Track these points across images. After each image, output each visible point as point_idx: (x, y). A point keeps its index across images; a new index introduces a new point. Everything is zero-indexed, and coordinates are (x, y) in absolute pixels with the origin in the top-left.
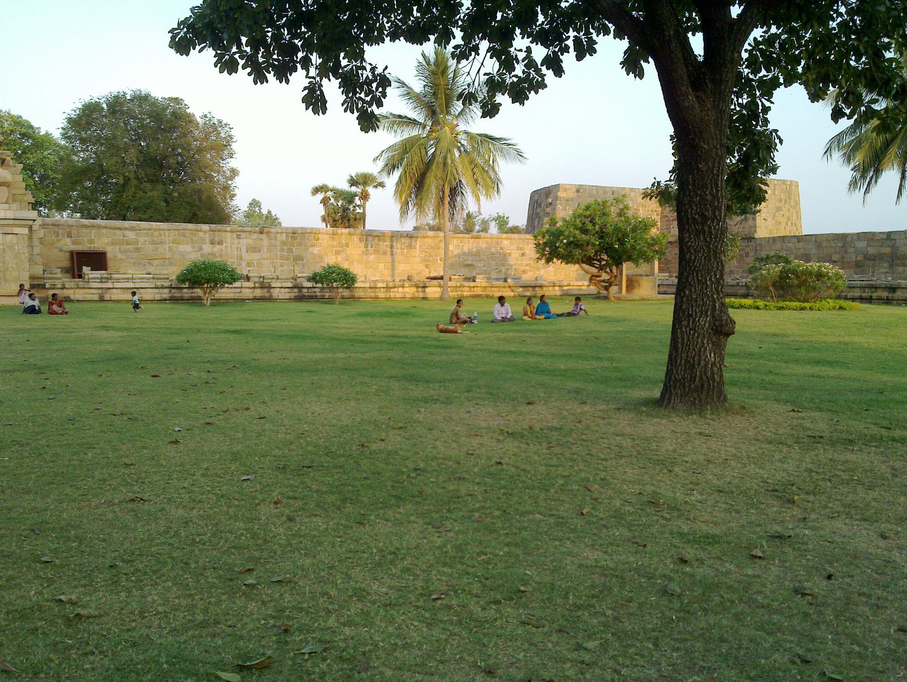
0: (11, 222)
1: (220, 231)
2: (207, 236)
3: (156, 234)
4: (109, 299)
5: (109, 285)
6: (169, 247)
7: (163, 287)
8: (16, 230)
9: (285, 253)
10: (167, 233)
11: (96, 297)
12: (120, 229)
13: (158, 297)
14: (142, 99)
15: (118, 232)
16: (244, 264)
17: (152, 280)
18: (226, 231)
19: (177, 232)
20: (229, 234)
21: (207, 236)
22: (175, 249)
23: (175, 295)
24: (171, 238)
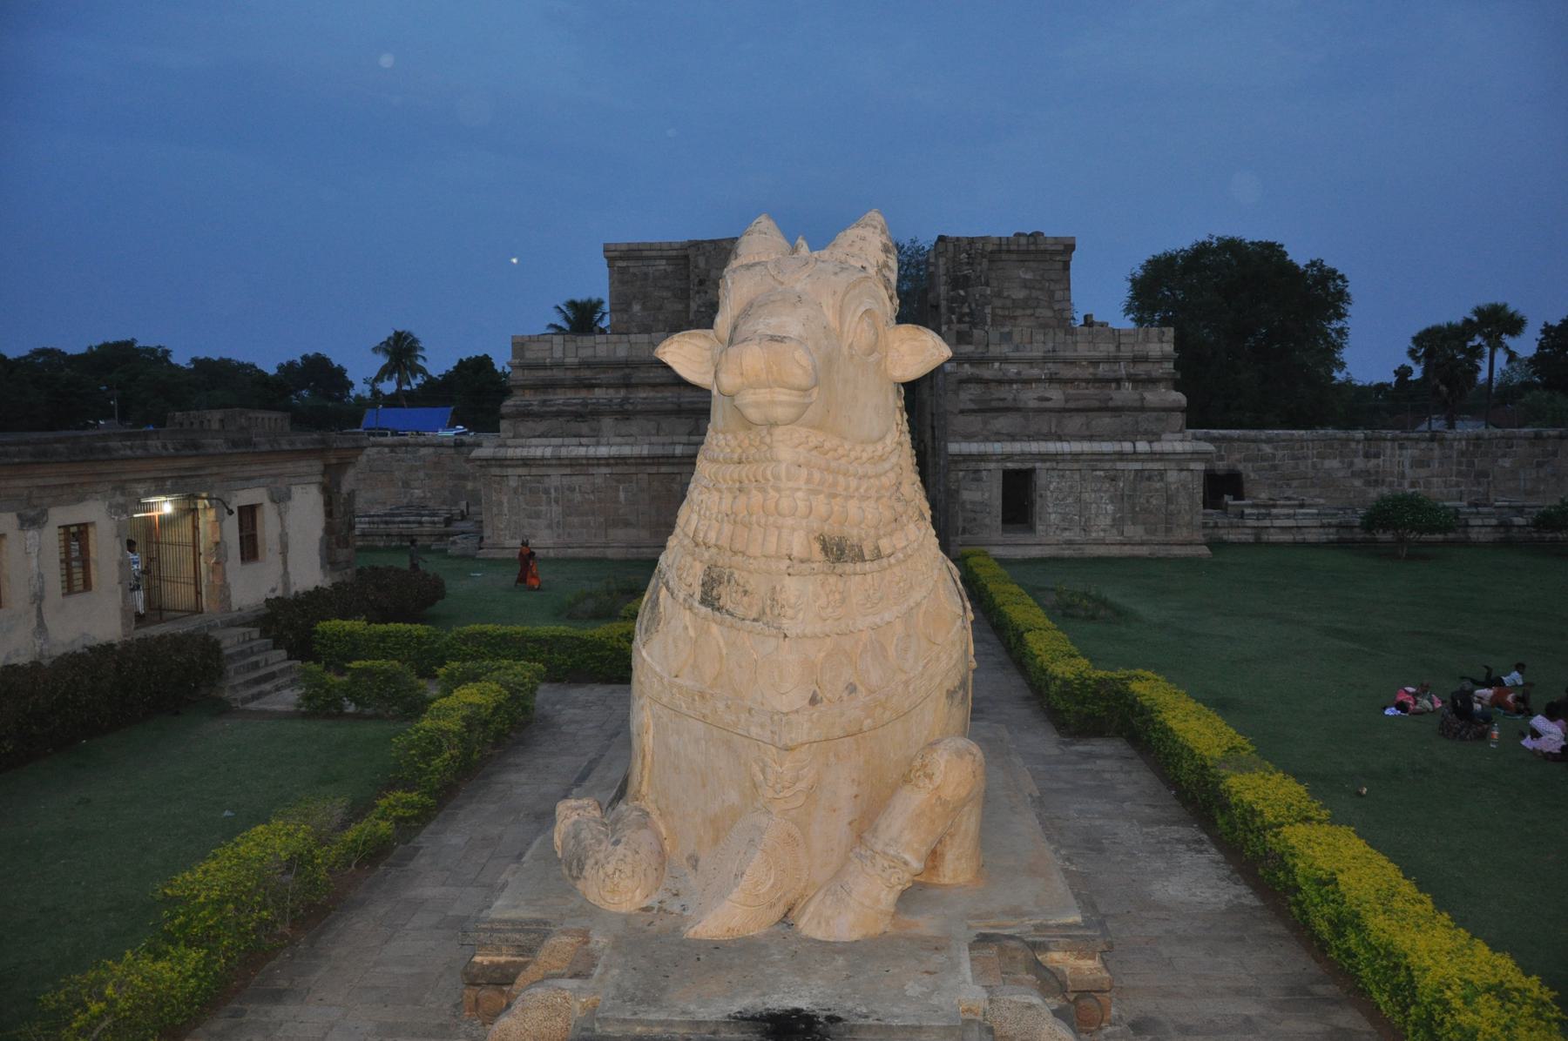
0: (1189, 456)
1: (1377, 439)
2: (1361, 446)
3: (1298, 445)
5: (1267, 523)
7: (1330, 526)
8: (1192, 466)
9: (1464, 468)
10: (1310, 444)
11: (1251, 539)
12: (1254, 441)
13: (1324, 538)
14: (1232, 246)
15: (1253, 446)
16: (1406, 484)
18: (1385, 440)
19: (1323, 444)
20: (1389, 444)
21: (1361, 446)
22: (1319, 466)
23: (1344, 536)
24: (1315, 452)
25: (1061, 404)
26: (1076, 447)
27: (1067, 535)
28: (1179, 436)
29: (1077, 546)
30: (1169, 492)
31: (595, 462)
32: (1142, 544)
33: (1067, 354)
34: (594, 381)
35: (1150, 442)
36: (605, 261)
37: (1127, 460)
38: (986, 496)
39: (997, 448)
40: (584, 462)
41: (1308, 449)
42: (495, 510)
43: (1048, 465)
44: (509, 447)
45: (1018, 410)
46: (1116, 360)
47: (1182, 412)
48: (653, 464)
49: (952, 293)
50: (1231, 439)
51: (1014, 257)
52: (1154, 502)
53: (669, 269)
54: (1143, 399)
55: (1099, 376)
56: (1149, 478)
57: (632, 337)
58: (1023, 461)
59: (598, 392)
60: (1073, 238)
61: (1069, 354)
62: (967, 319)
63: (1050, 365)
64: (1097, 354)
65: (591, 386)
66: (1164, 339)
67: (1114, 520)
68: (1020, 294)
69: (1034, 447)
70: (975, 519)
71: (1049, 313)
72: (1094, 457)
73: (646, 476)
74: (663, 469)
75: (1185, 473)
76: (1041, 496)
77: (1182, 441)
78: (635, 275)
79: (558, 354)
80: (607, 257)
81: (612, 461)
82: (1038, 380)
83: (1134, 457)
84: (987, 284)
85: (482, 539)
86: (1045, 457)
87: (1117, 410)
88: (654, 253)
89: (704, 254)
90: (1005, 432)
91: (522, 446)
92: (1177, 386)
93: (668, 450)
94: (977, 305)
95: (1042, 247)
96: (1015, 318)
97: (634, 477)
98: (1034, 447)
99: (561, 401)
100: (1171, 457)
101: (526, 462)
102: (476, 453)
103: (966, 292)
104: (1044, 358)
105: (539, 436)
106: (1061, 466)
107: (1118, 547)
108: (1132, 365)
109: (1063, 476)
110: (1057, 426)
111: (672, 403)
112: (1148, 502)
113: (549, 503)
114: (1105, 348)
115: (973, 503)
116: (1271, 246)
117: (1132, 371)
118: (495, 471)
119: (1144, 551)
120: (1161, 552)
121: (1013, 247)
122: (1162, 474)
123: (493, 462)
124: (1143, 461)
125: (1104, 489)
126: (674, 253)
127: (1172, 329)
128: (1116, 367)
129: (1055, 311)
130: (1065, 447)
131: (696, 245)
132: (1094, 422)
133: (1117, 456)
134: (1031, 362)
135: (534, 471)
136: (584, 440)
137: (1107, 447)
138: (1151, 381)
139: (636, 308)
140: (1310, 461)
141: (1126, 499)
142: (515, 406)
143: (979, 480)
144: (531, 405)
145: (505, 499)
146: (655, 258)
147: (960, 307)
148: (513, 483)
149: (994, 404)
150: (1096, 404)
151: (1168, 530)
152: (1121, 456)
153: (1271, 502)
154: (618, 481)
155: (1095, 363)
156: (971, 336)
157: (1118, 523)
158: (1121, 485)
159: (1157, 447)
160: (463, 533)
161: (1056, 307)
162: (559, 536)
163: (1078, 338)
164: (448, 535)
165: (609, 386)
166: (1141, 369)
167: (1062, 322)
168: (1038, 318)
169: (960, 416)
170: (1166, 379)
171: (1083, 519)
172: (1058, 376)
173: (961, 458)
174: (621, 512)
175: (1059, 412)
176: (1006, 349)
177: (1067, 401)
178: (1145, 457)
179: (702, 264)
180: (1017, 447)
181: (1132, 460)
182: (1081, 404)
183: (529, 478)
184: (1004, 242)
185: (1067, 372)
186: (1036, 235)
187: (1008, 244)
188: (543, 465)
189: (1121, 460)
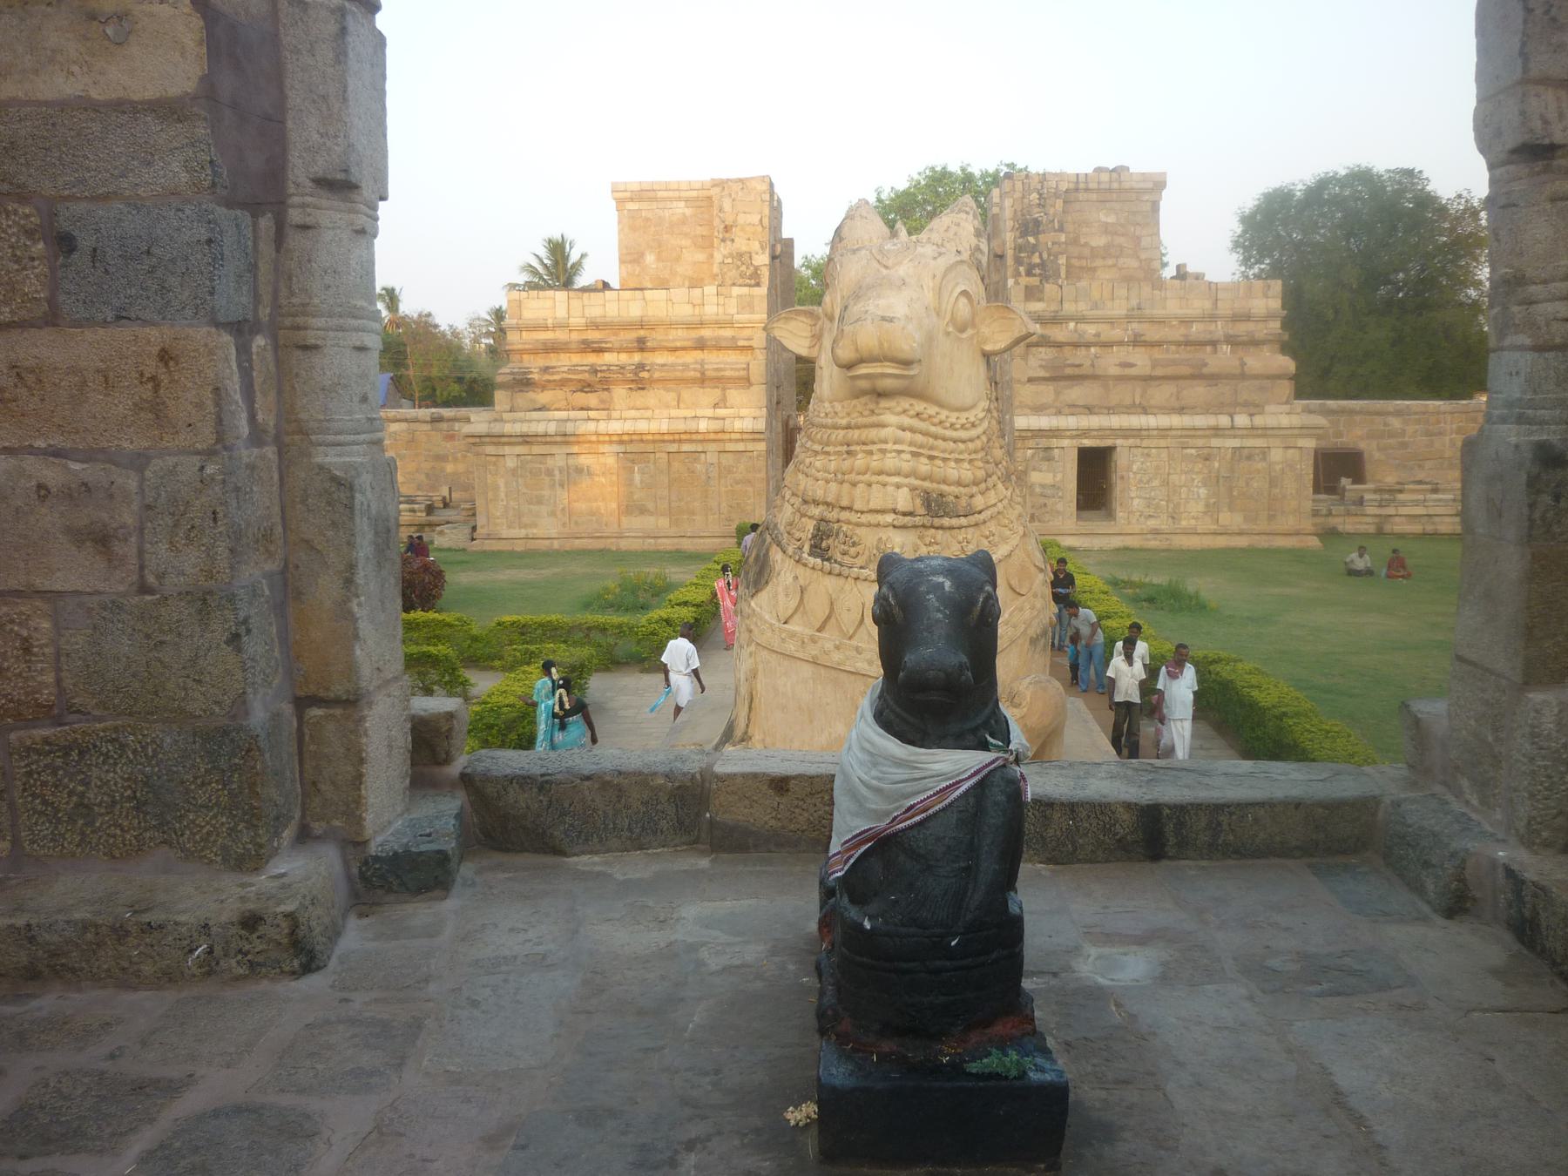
0: (1296, 432)
4: (1390, 531)
6: (1451, 440)
8: (1301, 443)
10: (1449, 417)
12: (1378, 413)
15: (1378, 419)
17: (1450, 503)
19: (1464, 416)
24: (1454, 426)
25: (1147, 371)
26: (1164, 421)
27: (1152, 523)
28: (1286, 408)
29: (1164, 536)
30: (1273, 474)
31: (607, 438)
32: (1240, 534)
33: (1155, 312)
34: (604, 345)
35: (1251, 415)
36: (614, 203)
37: (1223, 436)
38: (1059, 476)
39: (1070, 422)
40: (594, 438)
41: (1445, 423)
42: (490, 495)
43: (1131, 442)
44: (506, 422)
45: (1095, 377)
46: (1213, 318)
47: (1291, 379)
48: (674, 441)
49: (1020, 241)
50: (1352, 412)
51: (1094, 196)
52: (1255, 485)
53: (688, 212)
54: (1243, 364)
55: (1191, 338)
56: (1249, 458)
57: (648, 293)
58: (1102, 437)
59: (609, 358)
60: (1165, 174)
61: (1158, 312)
62: (1037, 271)
63: (1135, 326)
64: (1189, 312)
65: (601, 351)
66: (1270, 293)
67: (1207, 505)
68: (1099, 241)
69: (1116, 421)
70: (1045, 505)
71: (1134, 264)
72: (1185, 433)
73: (665, 456)
74: (686, 447)
75: (1291, 451)
76: (1122, 478)
77: (1288, 414)
78: (648, 219)
79: (561, 313)
80: (615, 199)
81: (626, 438)
82: (1120, 343)
83: (1232, 432)
84: (1061, 229)
85: (474, 529)
86: (1128, 433)
87: (1214, 378)
88: (671, 194)
89: (730, 195)
90: (1081, 403)
91: (522, 421)
92: (1285, 349)
93: (692, 426)
94: (1049, 255)
95: (1126, 186)
96: (1094, 270)
97: (652, 456)
98: (1116, 421)
99: (566, 369)
100: (1276, 432)
101: (526, 439)
102: (467, 429)
103: (1037, 239)
104: (1127, 317)
105: (540, 409)
106: (1145, 443)
107: (1211, 537)
108: (1230, 325)
109: (1148, 455)
110: (1142, 397)
111: (695, 370)
112: (1247, 484)
113: (552, 486)
114: (1200, 305)
115: (1043, 486)
116: (1409, 173)
117: (1231, 332)
118: (490, 449)
119: (1242, 542)
120: (1263, 542)
121: (1093, 185)
122: (1264, 452)
123: (487, 439)
124: (1242, 437)
125: (1196, 470)
126: (694, 194)
127: (1279, 282)
128: (1213, 327)
129: (1141, 261)
130: (1151, 421)
131: (720, 184)
132: (1185, 392)
133: (1212, 432)
134: (1111, 322)
135: (536, 449)
136: (592, 414)
137: (1200, 421)
138: (1255, 343)
139: (650, 258)
140: (1447, 438)
141: (1221, 480)
142: (512, 373)
143: (1049, 459)
144: (531, 372)
145: (501, 483)
146: (671, 200)
147: (1029, 257)
148: (511, 463)
149: (1069, 371)
150: (1186, 370)
151: (1271, 518)
152: (1217, 431)
153: (1398, 487)
154: (633, 461)
155: (1186, 322)
156: (1042, 291)
157: (1211, 509)
158: (1217, 465)
159: (1259, 421)
160: (448, 523)
161: (1143, 256)
162: (564, 525)
163: (1169, 294)
164: (431, 525)
165: (620, 350)
166: (1242, 329)
167: (1149, 274)
168: (1120, 269)
169: (1028, 385)
170: (1270, 341)
171: (1171, 505)
172: (1143, 338)
173: (1029, 434)
174: (635, 497)
175: (1145, 380)
176: (1082, 307)
177: (1153, 367)
178: (1245, 432)
179: (727, 205)
180: (1094, 421)
181: (1230, 436)
182: (1169, 371)
183: (530, 457)
184: (1082, 179)
185: (1153, 334)
186: (1119, 171)
187: (1086, 182)
188: (546, 443)
189: (1216, 436)
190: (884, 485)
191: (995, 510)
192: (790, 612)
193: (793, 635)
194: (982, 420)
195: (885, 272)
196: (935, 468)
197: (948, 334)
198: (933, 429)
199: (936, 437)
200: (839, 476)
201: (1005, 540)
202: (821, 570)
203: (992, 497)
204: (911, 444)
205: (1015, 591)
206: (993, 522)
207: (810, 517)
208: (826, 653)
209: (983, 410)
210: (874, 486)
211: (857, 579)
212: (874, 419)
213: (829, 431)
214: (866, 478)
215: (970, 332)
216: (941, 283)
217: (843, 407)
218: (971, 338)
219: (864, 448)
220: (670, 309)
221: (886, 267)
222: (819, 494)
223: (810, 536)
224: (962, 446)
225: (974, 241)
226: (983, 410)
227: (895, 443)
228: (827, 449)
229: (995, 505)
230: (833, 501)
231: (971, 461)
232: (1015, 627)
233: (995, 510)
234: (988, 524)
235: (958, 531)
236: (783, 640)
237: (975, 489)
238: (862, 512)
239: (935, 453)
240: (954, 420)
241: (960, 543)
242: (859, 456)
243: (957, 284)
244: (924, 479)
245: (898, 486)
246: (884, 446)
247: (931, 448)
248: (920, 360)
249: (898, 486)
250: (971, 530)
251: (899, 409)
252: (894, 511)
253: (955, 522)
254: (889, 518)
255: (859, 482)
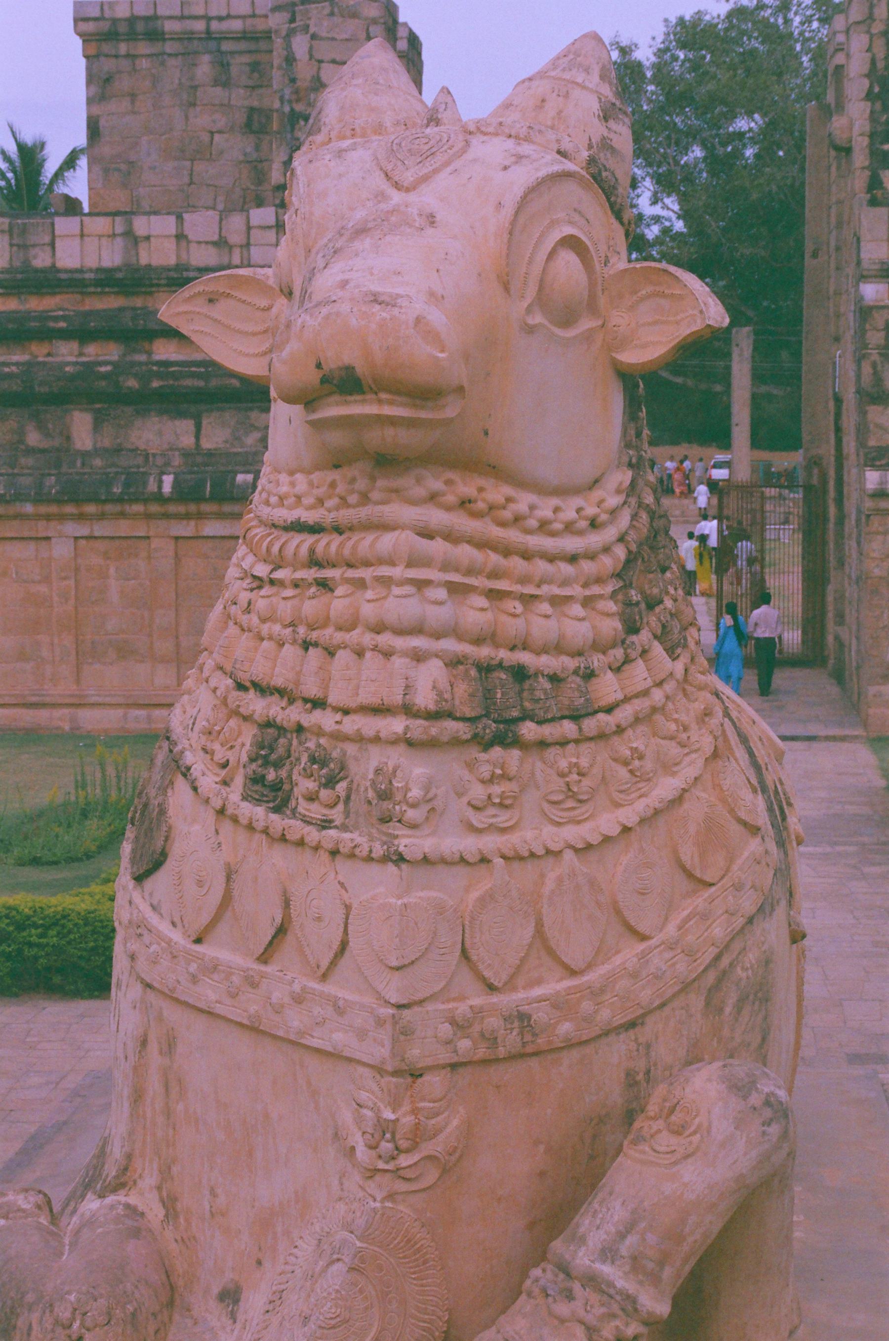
36: (78, 42)
65: (46, 335)
80: (80, 35)
190: (388, 654)
191: (640, 705)
192: (205, 919)
193: (213, 967)
194: (613, 512)
195: (397, 197)
196: (503, 618)
197: (530, 330)
198: (497, 532)
199: (507, 552)
200: (302, 630)
201: (668, 767)
202: (265, 831)
203: (639, 674)
204: (445, 567)
205: (690, 875)
206: (641, 729)
207: (246, 718)
208: (278, 1010)
209: (618, 491)
210: (368, 655)
211: (334, 853)
212: (364, 513)
213: (285, 536)
214: (355, 636)
215: (586, 324)
216: (513, 223)
217: (311, 484)
218: (588, 337)
219: (351, 573)
220: (184, 255)
221: (397, 186)
222: (258, 669)
223: (244, 758)
224: (566, 569)
225: (598, 130)
226: (618, 491)
227: (409, 565)
228: (279, 574)
229: (645, 693)
230: (291, 686)
231: (587, 602)
232: (690, 953)
233: (640, 705)
234: (630, 732)
235: (557, 750)
236: (194, 979)
237: (597, 661)
238: (346, 712)
239: (502, 585)
240: (548, 513)
241: (562, 775)
242: (340, 591)
243: (553, 223)
244: (478, 641)
245: (418, 657)
246: (385, 571)
247: (494, 575)
248: (460, 390)
249: (418, 657)
250: (585, 747)
251: (419, 492)
252: (408, 710)
253: (547, 731)
254: (397, 725)
255: (339, 647)
